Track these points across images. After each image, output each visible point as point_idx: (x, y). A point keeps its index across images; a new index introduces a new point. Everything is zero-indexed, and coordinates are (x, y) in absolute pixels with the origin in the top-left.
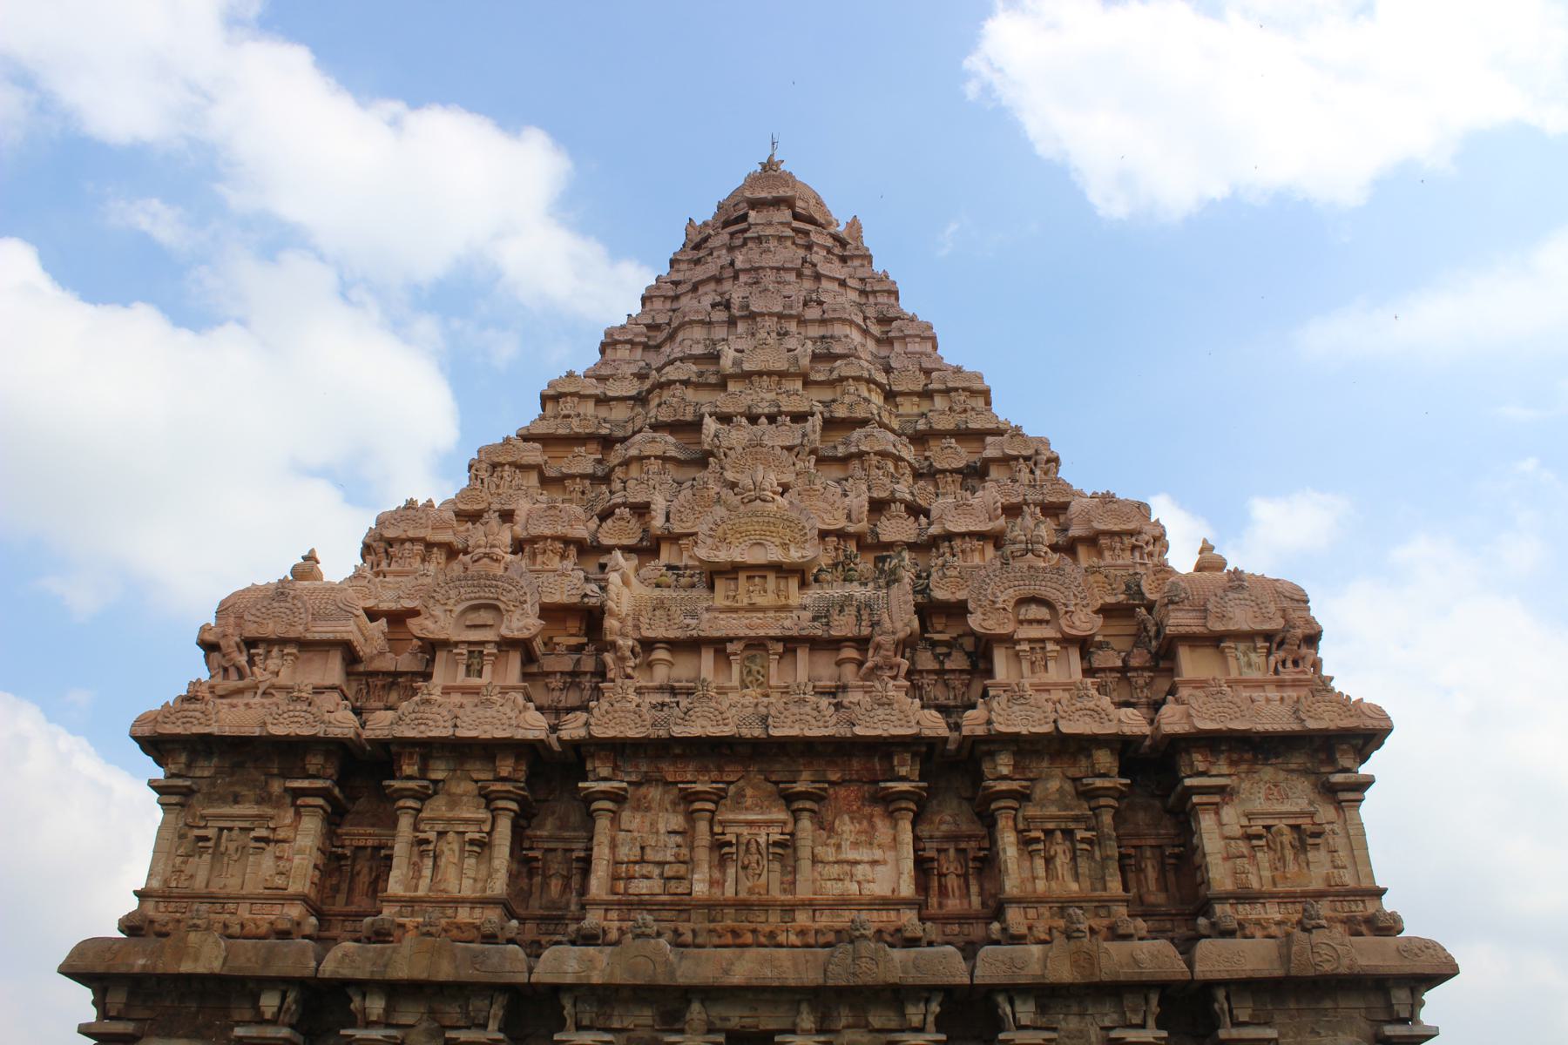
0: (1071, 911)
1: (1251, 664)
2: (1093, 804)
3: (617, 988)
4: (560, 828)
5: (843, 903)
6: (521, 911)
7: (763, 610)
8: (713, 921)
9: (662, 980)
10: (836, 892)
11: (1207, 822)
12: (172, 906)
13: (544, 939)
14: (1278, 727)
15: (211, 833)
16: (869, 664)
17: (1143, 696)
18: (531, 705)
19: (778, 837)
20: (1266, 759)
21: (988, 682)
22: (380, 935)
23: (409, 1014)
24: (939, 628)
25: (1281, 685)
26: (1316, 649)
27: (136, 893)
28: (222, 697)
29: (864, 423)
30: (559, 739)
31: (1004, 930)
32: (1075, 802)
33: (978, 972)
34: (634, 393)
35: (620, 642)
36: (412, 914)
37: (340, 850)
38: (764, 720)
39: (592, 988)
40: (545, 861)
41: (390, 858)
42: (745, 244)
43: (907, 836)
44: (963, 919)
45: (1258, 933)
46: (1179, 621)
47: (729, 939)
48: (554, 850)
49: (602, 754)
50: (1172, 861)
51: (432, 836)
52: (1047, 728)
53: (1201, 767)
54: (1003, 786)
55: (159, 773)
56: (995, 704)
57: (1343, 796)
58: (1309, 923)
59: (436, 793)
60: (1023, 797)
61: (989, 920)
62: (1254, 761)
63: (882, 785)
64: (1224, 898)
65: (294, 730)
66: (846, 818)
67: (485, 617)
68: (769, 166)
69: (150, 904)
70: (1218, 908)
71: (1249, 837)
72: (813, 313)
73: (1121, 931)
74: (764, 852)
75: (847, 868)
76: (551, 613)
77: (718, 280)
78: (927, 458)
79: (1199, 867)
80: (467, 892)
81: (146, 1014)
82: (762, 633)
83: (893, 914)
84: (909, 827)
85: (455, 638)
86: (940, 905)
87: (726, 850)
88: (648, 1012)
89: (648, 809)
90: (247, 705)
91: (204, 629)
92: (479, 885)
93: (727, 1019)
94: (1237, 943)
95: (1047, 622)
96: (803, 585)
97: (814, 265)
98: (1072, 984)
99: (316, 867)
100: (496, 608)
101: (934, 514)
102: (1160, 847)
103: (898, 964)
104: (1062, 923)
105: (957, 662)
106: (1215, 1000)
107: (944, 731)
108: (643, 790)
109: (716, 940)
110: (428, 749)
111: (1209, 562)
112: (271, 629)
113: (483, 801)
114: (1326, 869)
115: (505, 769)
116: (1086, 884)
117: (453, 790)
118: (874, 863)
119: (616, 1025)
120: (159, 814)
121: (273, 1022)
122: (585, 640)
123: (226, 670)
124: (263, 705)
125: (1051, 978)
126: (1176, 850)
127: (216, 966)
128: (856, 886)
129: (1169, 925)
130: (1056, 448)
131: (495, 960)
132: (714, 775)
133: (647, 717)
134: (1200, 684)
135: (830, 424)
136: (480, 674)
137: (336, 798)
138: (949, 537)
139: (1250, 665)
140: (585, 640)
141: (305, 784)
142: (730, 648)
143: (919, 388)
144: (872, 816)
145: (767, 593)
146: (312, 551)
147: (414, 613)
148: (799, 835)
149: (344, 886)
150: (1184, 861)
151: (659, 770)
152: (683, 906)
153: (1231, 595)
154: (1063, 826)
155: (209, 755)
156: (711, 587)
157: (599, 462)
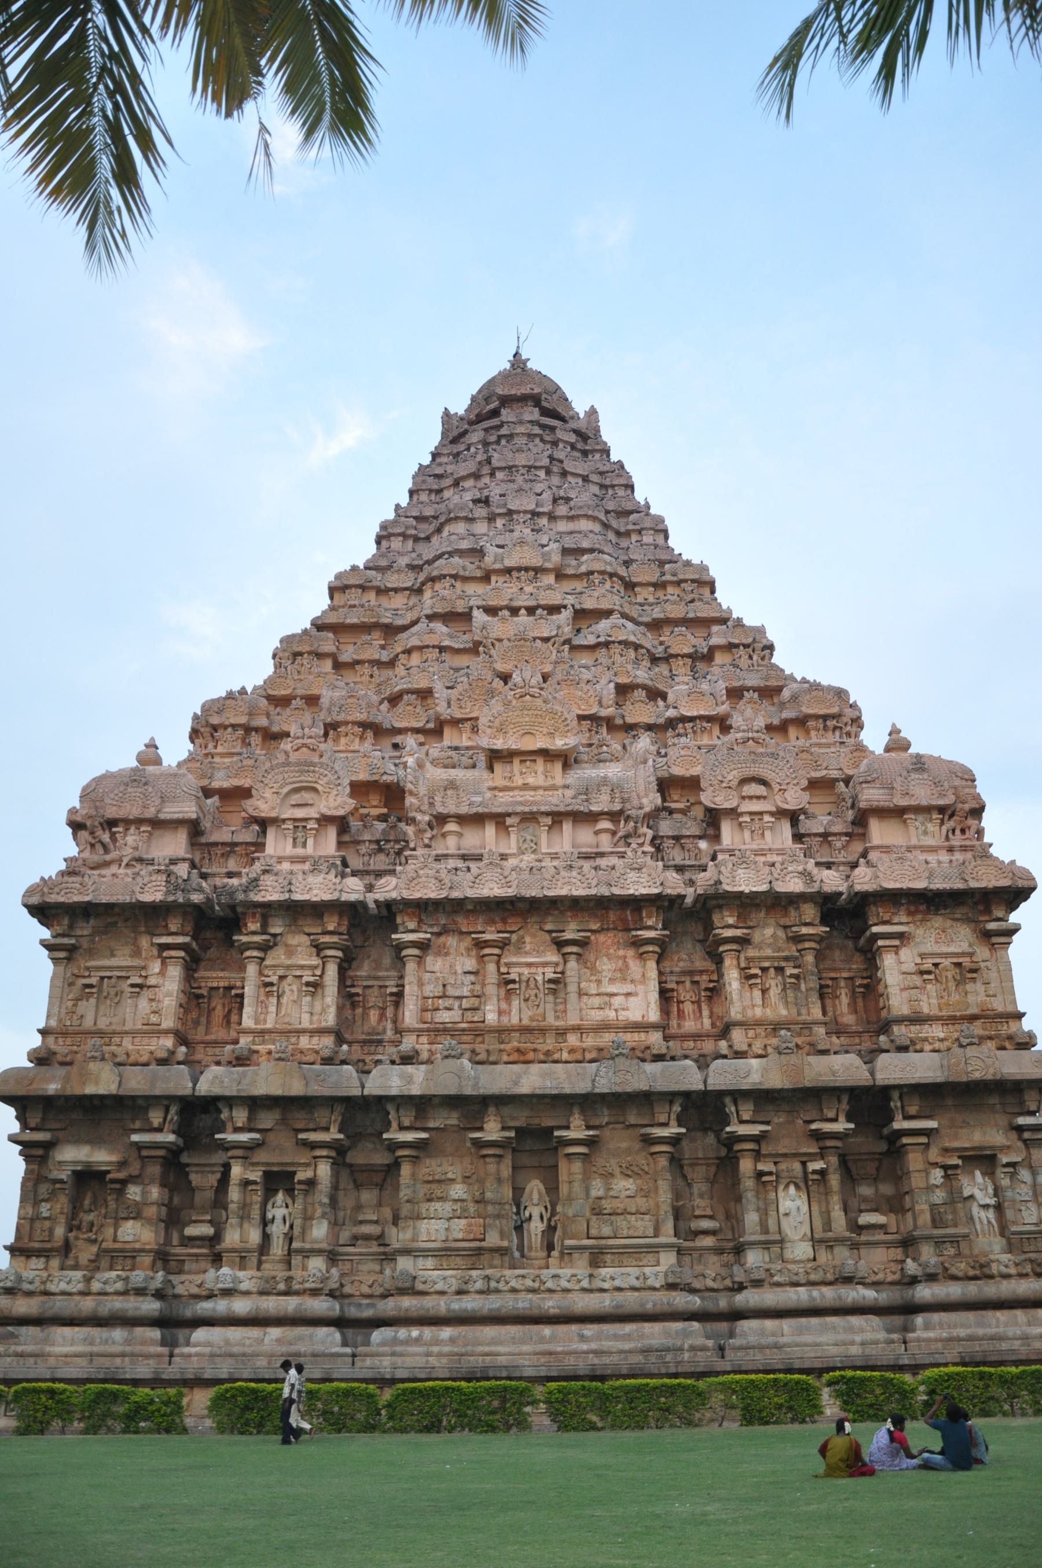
1: (930, 832)
2: (800, 947)
6: (347, 1036)
7: (535, 788)
8: (502, 1043)
9: (468, 1091)
10: (599, 1018)
11: (888, 961)
12: (69, 1041)
13: (368, 1058)
15: (93, 981)
16: (620, 834)
19: (552, 976)
20: (937, 910)
21: (717, 847)
22: (241, 1060)
23: (267, 1120)
24: (676, 797)
25: (951, 850)
26: (980, 819)
27: (39, 1031)
28: (92, 868)
29: (608, 613)
31: (730, 1046)
32: (785, 945)
33: (710, 1081)
34: (409, 584)
35: (419, 817)
36: (263, 1042)
39: (411, 1098)
40: (364, 996)
41: (241, 996)
42: (498, 442)
44: (696, 1037)
46: (871, 796)
47: (515, 1057)
49: (410, 910)
51: (274, 979)
52: (764, 888)
54: (729, 933)
55: (46, 934)
57: (995, 940)
59: (275, 944)
60: (744, 941)
62: (928, 912)
63: (634, 933)
64: (901, 1020)
66: (605, 959)
67: (307, 797)
68: (518, 362)
69: (51, 1040)
70: (895, 1029)
71: (922, 973)
72: (562, 510)
73: (820, 1047)
75: (607, 999)
76: (358, 789)
77: (476, 476)
78: (661, 643)
80: (306, 1024)
81: (57, 1125)
82: (535, 809)
83: (643, 1036)
84: (654, 965)
85: (284, 816)
86: (679, 1026)
88: (455, 1115)
89: (447, 954)
91: (72, 811)
94: (912, 1056)
95: (765, 798)
96: (566, 766)
98: (782, 1090)
99: (181, 1006)
100: (315, 790)
101: (671, 697)
102: (851, 978)
104: (774, 1041)
105: (692, 829)
106: (889, 1099)
107: (681, 890)
108: (442, 939)
109: (505, 1058)
111: (897, 744)
112: (134, 812)
113: (314, 950)
114: (981, 998)
118: (628, 995)
119: (431, 1125)
120: (48, 967)
121: (159, 1130)
122: (385, 811)
123: (92, 846)
124: (127, 875)
125: (767, 1086)
129: (857, 1040)
130: (771, 635)
131: (334, 1078)
132: (500, 926)
133: (446, 881)
134: (886, 849)
135: (580, 614)
136: (304, 845)
137: (193, 950)
138: (684, 719)
139: (925, 833)
140: (385, 811)
142: (509, 821)
143: (654, 580)
144: (625, 957)
145: (537, 774)
146: (152, 739)
148: (568, 973)
149: (203, 1020)
150: (869, 989)
151: (455, 923)
152: (478, 1031)
153: (914, 776)
156: (491, 768)
157: (383, 647)
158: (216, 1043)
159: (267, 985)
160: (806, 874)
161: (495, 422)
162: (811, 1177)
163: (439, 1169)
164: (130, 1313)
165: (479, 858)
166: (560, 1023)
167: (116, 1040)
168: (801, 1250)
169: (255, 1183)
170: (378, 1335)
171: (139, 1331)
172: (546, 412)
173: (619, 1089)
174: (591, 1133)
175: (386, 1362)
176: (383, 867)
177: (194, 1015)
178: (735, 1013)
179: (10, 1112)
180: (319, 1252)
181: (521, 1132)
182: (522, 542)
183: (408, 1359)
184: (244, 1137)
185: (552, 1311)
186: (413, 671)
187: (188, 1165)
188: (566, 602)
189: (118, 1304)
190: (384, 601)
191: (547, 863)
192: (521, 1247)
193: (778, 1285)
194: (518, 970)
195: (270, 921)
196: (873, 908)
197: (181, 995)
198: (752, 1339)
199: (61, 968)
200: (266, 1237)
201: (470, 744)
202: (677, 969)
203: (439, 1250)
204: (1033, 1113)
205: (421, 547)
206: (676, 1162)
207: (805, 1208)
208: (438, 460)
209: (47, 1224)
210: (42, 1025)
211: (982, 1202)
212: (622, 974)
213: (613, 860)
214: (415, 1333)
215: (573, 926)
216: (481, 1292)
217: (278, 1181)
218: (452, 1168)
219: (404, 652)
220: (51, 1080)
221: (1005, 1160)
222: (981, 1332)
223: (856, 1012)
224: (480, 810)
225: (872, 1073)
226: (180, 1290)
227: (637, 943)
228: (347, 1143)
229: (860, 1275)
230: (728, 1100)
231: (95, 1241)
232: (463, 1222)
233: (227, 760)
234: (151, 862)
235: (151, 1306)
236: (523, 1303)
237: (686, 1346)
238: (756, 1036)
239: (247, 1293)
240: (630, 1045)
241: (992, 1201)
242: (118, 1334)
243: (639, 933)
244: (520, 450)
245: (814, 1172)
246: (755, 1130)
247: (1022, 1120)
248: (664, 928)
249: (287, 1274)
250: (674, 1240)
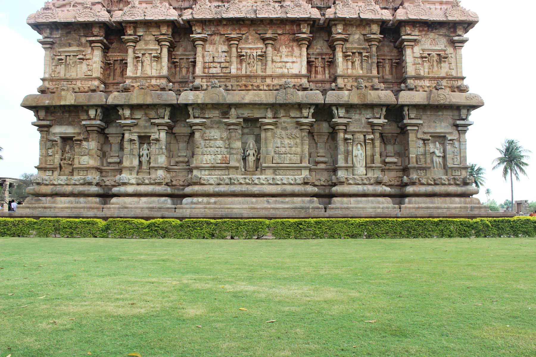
0: (359, 80)
2: (370, 44)
3: (207, 104)
4: (185, 51)
5: (282, 76)
6: (173, 80)
9: (221, 101)
12: (54, 83)
13: (181, 89)
14: (438, 19)
15: (63, 57)
17: (391, 6)
18: (171, 7)
19: (260, 53)
20: (432, 30)
22: (126, 90)
23: (139, 114)
30: (182, 19)
32: (363, 43)
33: (326, 99)
36: (136, 82)
37: (109, 62)
38: (255, 11)
39: (198, 104)
41: (126, 63)
43: (305, 53)
44: (322, 82)
45: (421, 90)
47: (243, 88)
48: (183, 59)
50: (395, 64)
51: (140, 55)
52: (356, 16)
53: (409, 32)
54: (339, 36)
56: (338, 7)
57: (457, 45)
58: (438, 87)
59: (140, 40)
60: (346, 40)
61: (331, 82)
62: (428, 31)
63: (297, 35)
64: (411, 78)
65: (86, 19)
66: (284, 47)
70: (409, 81)
71: (422, 58)
73: (375, 87)
74: (255, 58)
75: (284, 64)
79: (404, 67)
83: (299, 79)
84: (305, 50)
86: (315, 77)
87: (242, 58)
88: (217, 112)
89: (215, 44)
90: (68, 10)
92: (158, 72)
93: (244, 114)
98: (356, 105)
99: (101, 67)
102: (391, 59)
103: (300, 97)
104: (356, 84)
106: (404, 111)
107: (319, 16)
108: (213, 37)
109: (239, 88)
110: (136, 24)
115: (164, 30)
116: (365, 71)
118: (293, 62)
119: (207, 116)
121: (94, 119)
124: (74, 10)
126: (397, 61)
127: (73, 102)
128: (287, 70)
129: (391, 86)
132: (238, 31)
133: (213, 10)
137: (105, 43)
141: (94, 39)
144: (293, 46)
148: (267, 52)
149: (112, 74)
150: (399, 64)
151: (218, 30)
152: (228, 77)
154: (359, 51)
155: (57, 29)
162: (367, 141)
164: (86, 192)
168: (361, 170)
169: (134, 140)
170: (185, 200)
171: (90, 198)
174: (275, 120)
175: (188, 211)
177: (108, 72)
179: (31, 113)
180: (161, 168)
181: (246, 120)
183: (197, 210)
184: (128, 122)
185: (256, 192)
187: (108, 134)
189: (81, 188)
192: (245, 167)
193: (350, 184)
195: (138, 30)
198: (338, 205)
199: (48, 52)
200: (140, 162)
202: (315, 53)
203: (211, 167)
204: (464, 120)
206: (311, 134)
209: (51, 158)
210: (42, 77)
211: (438, 155)
214: (200, 199)
216: (227, 184)
217: (144, 139)
218: (215, 133)
221: (449, 138)
222: (431, 205)
223: (392, 74)
225: (397, 99)
226: (107, 183)
228: (172, 123)
229: (384, 181)
230: (334, 109)
235: (94, 189)
236: (244, 188)
237: (311, 207)
239: (132, 184)
241: (441, 155)
242: (82, 199)
245: (369, 139)
247: (458, 122)
248: (311, 33)
249: (149, 177)
250: (309, 165)
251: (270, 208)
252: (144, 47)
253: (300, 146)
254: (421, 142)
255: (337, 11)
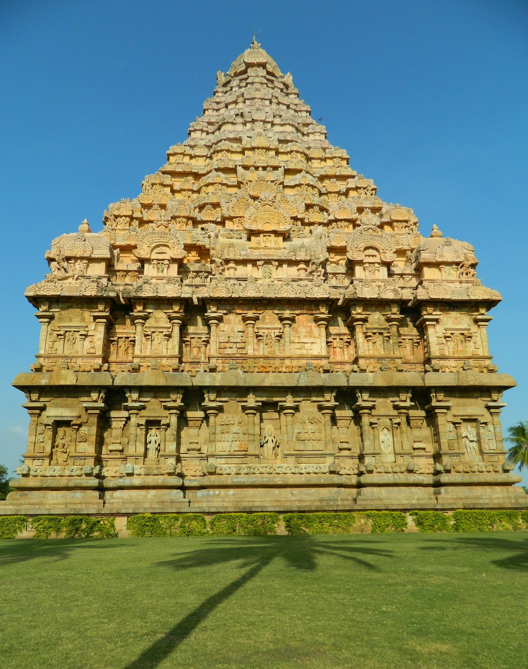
7: (270, 249)
8: (255, 363)
9: (241, 384)
10: (299, 353)
11: (431, 331)
12: (50, 361)
13: (193, 370)
19: (278, 334)
25: (461, 282)
28: (59, 280)
29: (300, 171)
33: (350, 382)
34: (205, 154)
35: (217, 260)
41: (134, 341)
43: (324, 334)
44: (342, 363)
46: (425, 257)
51: (150, 333)
53: (430, 312)
57: (480, 323)
60: (365, 320)
63: (316, 315)
66: (302, 327)
70: (433, 362)
71: (445, 337)
72: (277, 121)
74: (273, 339)
75: (303, 344)
78: (324, 187)
80: (165, 354)
85: (152, 258)
86: (334, 358)
87: (259, 338)
89: (230, 323)
96: (284, 240)
97: (277, 98)
100: (168, 246)
108: (228, 316)
117: (157, 316)
121: (96, 401)
122: (199, 258)
123: (59, 269)
129: (414, 367)
133: (231, 289)
134: (432, 281)
135: (288, 172)
137: (110, 319)
138: (336, 220)
139: (449, 274)
140: (199, 258)
142: (258, 263)
144: (311, 326)
147: (135, 247)
148: (285, 333)
152: (245, 358)
153: (446, 247)
154: (379, 331)
156: (249, 239)
157: (194, 183)
158: (121, 363)
159: (146, 336)
160: (394, 291)
161: (245, 76)
163: (227, 419)
165: (245, 280)
166: (282, 355)
167: (74, 360)
168: (391, 458)
169: (142, 425)
172: (268, 73)
173: (309, 385)
174: (296, 404)
176: (199, 284)
178: (361, 353)
179: (22, 394)
182: (260, 135)
186: (210, 194)
188: (280, 165)
190: (193, 161)
191: (276, 282)
194: (263, 331)
196: (424, 308)
197: (105, 340)
200: (146, 449)
201: (238, 228)
204: (495, 401)
205: (210, 136)
207: (391, 439)
208: (217, 94)
211: (471, 440)
212: (310, 334)
213: (306, 282)
214: (217, 491)
215: (288, 312)
219: (205, 186)
220: (44, 378)
222: (470, 495)
224: (245, 258)
227: (316, 320)
230: (357, 391)
231: (66, 453)
232: (238, 443)
233: (122, 232)
234: (89, 278)
237: (339, 499)
238: (371, 363)
240: (315, 365)
243: (318, 315)
244: (257, 90)
245: (396, 424)
246: (370, 404)
251: (295, 501)
252: (154, 324)
253: (323, 432)
254: (452, 426)
255: (357, 292)
